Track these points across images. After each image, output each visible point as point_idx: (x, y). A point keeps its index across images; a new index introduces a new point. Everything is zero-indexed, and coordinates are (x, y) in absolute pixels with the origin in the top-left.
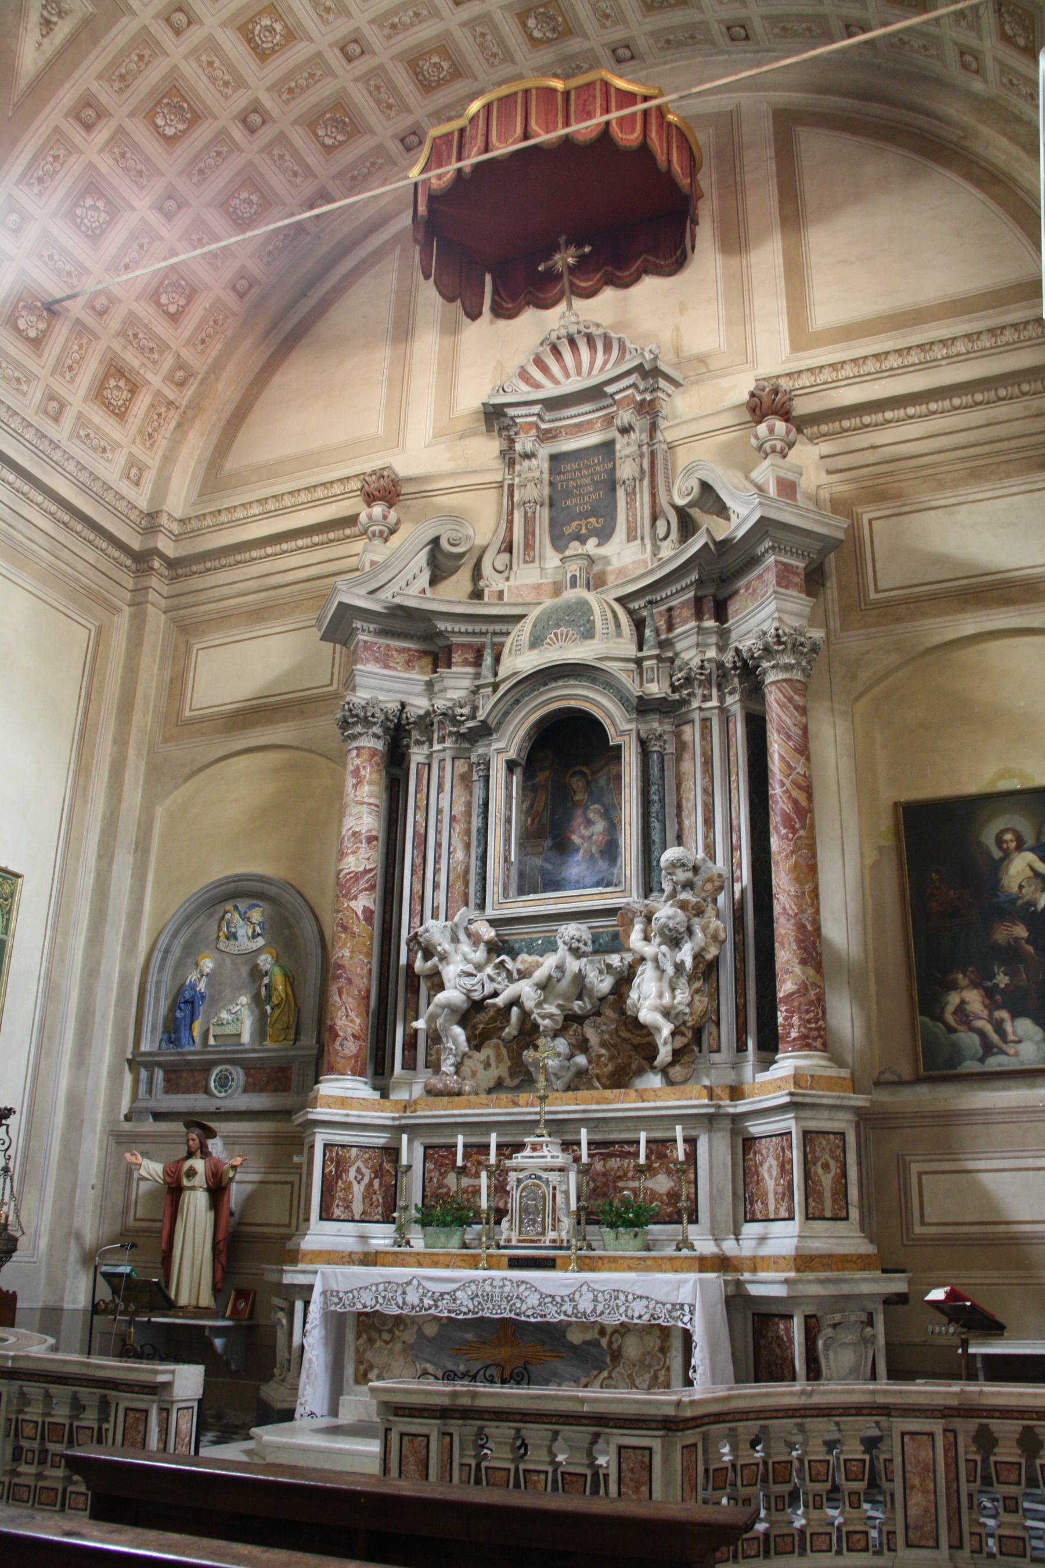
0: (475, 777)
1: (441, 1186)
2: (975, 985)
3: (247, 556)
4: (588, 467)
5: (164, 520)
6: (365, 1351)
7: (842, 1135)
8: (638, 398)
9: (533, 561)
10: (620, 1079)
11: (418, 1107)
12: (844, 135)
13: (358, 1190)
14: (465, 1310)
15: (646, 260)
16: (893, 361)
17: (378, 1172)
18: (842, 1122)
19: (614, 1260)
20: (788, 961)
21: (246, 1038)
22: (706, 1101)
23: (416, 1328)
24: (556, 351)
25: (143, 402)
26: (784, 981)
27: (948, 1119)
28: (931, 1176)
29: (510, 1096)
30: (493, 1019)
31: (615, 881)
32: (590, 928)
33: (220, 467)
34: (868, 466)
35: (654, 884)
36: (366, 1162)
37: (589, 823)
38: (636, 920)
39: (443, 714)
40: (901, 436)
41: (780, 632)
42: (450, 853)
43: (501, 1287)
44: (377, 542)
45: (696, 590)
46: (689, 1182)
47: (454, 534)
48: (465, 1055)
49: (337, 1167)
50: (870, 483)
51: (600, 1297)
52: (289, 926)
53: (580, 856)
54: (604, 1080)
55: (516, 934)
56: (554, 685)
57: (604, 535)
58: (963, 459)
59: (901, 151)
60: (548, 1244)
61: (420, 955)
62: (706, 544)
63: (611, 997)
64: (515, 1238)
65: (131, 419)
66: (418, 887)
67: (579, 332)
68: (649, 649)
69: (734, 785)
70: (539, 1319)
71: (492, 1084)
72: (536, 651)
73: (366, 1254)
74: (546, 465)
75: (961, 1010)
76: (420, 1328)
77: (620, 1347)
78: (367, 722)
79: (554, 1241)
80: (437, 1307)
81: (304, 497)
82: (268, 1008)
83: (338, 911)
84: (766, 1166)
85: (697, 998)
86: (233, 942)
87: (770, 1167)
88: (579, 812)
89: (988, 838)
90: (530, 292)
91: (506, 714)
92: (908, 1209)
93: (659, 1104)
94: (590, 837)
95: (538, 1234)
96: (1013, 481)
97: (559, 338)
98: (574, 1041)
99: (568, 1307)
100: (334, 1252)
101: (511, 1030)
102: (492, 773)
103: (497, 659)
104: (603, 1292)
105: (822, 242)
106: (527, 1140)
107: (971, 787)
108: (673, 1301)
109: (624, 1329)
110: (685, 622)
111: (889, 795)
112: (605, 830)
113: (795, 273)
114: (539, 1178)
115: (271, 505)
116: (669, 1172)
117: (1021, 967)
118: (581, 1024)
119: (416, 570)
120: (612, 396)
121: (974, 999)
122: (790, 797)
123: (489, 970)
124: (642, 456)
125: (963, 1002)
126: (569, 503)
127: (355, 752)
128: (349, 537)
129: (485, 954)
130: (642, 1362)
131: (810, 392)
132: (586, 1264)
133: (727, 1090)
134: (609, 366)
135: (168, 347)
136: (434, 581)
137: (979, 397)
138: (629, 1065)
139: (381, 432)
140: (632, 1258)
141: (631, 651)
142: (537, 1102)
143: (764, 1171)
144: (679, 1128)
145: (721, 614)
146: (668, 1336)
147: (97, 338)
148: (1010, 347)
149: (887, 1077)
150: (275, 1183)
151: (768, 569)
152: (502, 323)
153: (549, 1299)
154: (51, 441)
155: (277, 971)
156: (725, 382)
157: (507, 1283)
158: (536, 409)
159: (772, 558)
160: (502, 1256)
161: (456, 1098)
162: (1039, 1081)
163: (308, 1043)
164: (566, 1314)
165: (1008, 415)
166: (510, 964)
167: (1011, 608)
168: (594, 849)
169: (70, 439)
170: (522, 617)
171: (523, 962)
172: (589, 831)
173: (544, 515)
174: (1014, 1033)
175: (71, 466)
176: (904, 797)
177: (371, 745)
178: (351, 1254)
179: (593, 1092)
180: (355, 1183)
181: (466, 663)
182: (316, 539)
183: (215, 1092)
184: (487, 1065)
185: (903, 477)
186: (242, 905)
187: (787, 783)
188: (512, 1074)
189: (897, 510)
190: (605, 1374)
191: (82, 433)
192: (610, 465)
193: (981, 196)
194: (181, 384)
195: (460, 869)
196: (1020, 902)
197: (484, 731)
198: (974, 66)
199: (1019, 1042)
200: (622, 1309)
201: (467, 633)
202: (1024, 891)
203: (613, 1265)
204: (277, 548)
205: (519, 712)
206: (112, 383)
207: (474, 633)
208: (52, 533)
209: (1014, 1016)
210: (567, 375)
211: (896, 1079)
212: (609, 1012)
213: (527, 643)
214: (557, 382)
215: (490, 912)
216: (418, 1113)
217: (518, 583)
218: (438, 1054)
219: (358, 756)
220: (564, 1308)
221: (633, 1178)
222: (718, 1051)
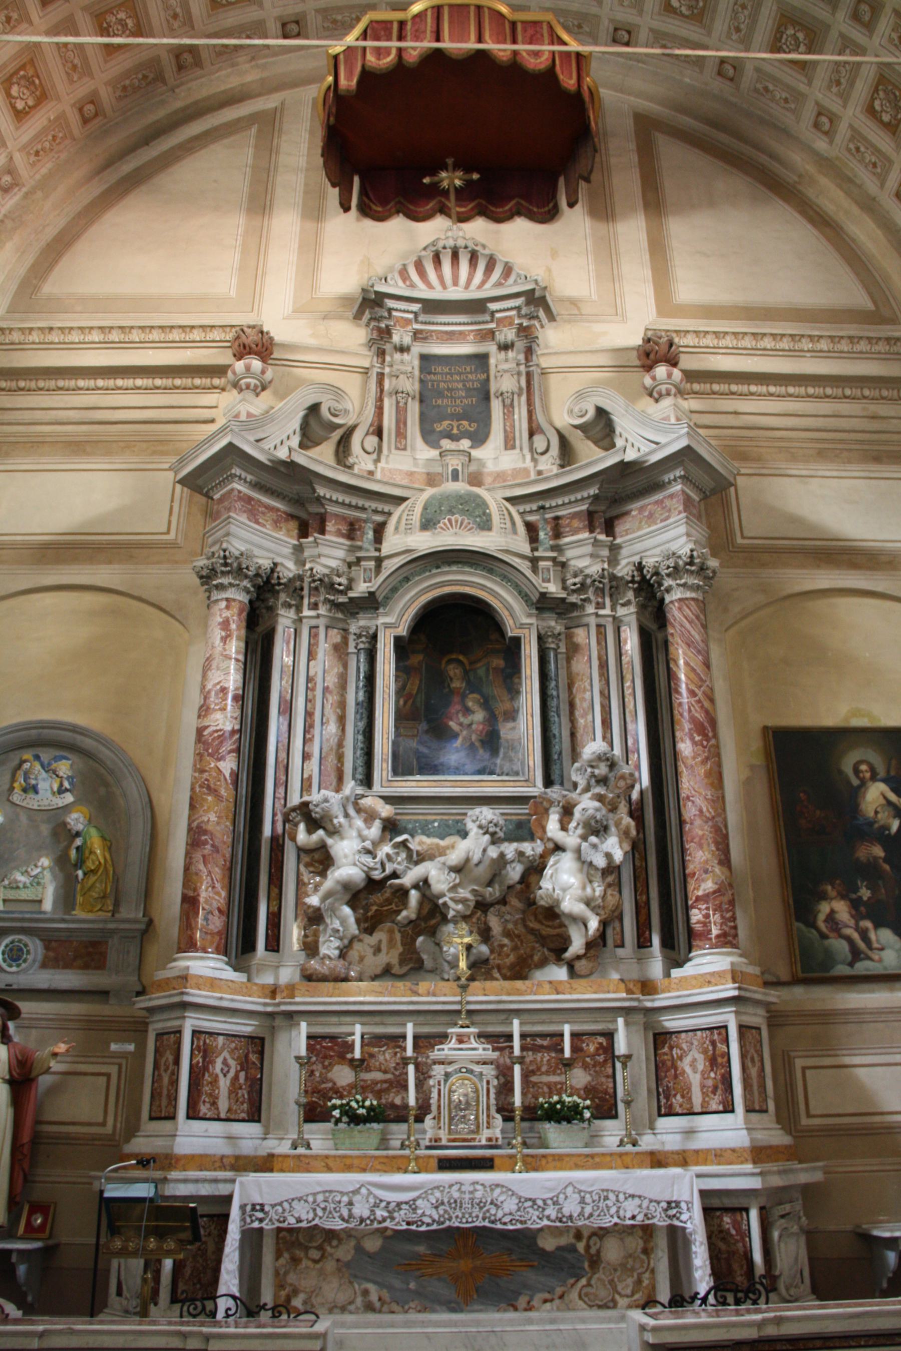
0: (351, 649)
1: (324, 1080)
2: (843, 897)
3: (72, 383)
4: (460, 374)
6: (286, 1273)
7: (758, 1029)
10: (519, 971)
11: (297, 992)
12: (697, 151)
13: (224, 1084)
14: (427, 1220)
15: (518, 203)
16: (767, 343)
17: (245, 1064)
19: (559, 1158)
20: (706, 862)
21: (48, 905)
22: (624, 995)
23: (353, 1243)
24: (437, 259)
27: (827, 1017)
28: (813, 1071)
29: (408, 984)
30: (388, 901)
31: (498, 771)
32: (502, 814)
33: (37, 288)
34: (732, 428)
35: (555, 777)
36: (232, 1052)
37: (467, 711)
38: (552, 810)
39: (320, 580)
40: (759, 408)
41: (695, 553)
42: (322, 724)
43: (471, 1192)
44: (249, 395)
45: (590, 504)
46: (608, 1077)
49: (204, 1058)
50: (733, 443)
51: (588, 1199)
52: (106, 785)
53: (458, 743)
54: (504, 971)
55: (411, 814)
56: (447, 569)
57: (480, 438)
58: (817, 440)
59: (749, 179)
60: (484, 1142)
61: (302, 827)
63: (519, 886)
64: (444, 1135)
67: (466, 247)
68: (545, 550)
69: (628, 692)
70: (519, 1226)
71: (378, 971)
73: (237, 1158)
74: (416, 363)
75: (831, 917)
76: (359, 1243)
77: (598, 1252)
78: (239, 572)
79: (490, 1139)
80: (393, 1219)
81: (155, 335)
83: (202, 771)
84: (687, 1060)
85: (609, 892)
86: (31, 795)
88: (456, 699)
89: (847, 766)
90: (400, 202)
91: (394, 590)
92: (795, 1103)
93: (575, 996)
94: (470, 725)
95: (473, 1132)
96: (854, 467)
97: (444, 248)
99: (551, 1211)
100: (206, 1156)
101: (409, 912)
102: (380, 645)
103: (378, 537)
104: (591, 1193)
105: (681, 230)
106: (450, 1031)
107: (829, 720)
108: (668, 1199)
109: (601, 1233)
110: (576, 532)
111: (758, 720)
113: (658, 249)
114: (470, 1071)
115: (115, 336)
116: (585, 1067)
117: (880, 882)
118: (485, 912)
120: (493, 313)
121: (842, 909)
122: (702, 707)
125: (832, 912)
126: (439, 402)
127: (223, 604)
128: (197, 388)
129: (380, 832)
130: (623, 1265)
131: (695, 351)
132: (533, 1164)
133: (639, 985)
134: (488, 285)
136: (302, 446)
137: (829, 391)
138: (532, 956)
139: (233, 293)
140: (579, 1155)
141: (525, 548)
142: (459, 990)
143: (685, 1065)
144: (516, 1022)
145: (609, 530)
146: (651, 1236)
148: (862, 356)
150: (93, 1074)
151: (671, 496)
152: (368, 223)
153: (530, 1203)
155: (93, 832)
157: (478, 1187)
158: (416, 307)
159: (679, 487)
160: (430, 1157)
162: (898, 985)
163: (132, 916)
164: (548, 1218)
165: (850, 412)
167: (859, 572)
168: (474, 737)
171: (421, 843)
172: (468, 720)
173: (414, 410)
174: (878, 941)
177: (241, 599)
178: (223, 1157)
179: (495, 983)
180: (221, 1076)
181: (339, 533)
182: (158, 382)
184: (377, 950)
185: (762, 444)
186: (46, 755)
187: (700, 693)
188: (402, 962)
189: (757, 471)
190: (583, 1281)
192: (484, 376)
193: (815, 232)
195: (334, 741)
196: (876, 826)
197: (372, 603)
198: (826, 127)
199: (882, 949)
200: (613, 1210)
201: (343, 504)
202: (879, 816)
203: (558, 1164)
204: (111, 383)
205: (408, 590)
207: (350, 506)
209: (877, 925)
210: (455, 283)
211: (775, 980)
212: (514, 902)
213: (418, 524)
216: (297, 999)
217: (391, 466)
218: (316, 935)
219: (227, 607)
220: (547, 1213)
221: (547, 1073)
222: (622, 946)
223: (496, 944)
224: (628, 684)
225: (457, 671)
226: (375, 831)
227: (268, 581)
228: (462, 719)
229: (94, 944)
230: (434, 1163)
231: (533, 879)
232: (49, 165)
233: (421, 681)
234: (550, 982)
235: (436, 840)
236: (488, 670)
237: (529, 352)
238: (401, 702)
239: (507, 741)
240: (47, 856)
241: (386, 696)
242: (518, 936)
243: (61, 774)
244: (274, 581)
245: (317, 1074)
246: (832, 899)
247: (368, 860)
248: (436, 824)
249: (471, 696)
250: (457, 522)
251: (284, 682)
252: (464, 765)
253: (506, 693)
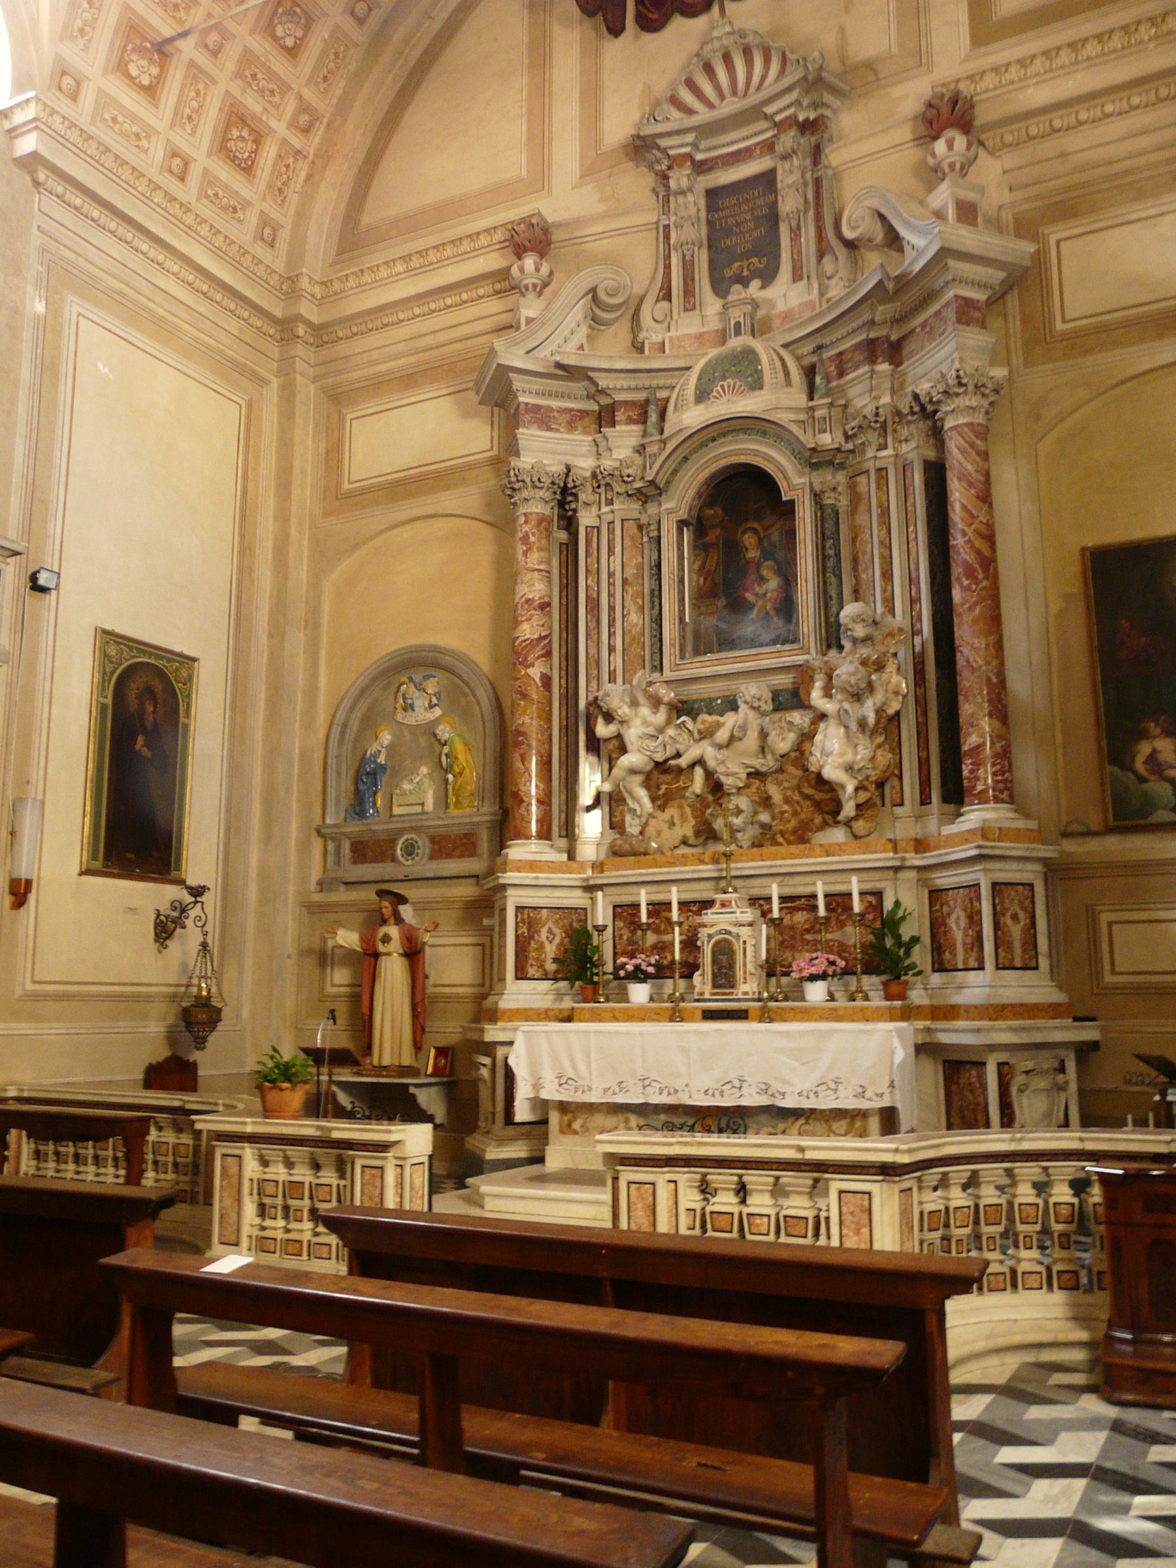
5: (305, 283)
7: (1031, 886)
8: (801, 118)
9: (694, 309)
10: (801, 836)
11: (605, 867)
18: (1030, 873)
22: (891, 854)
25: (270, 151)
26: (969, 734)
33: (357, 222)
37: (762, 580)
41: (961, 373)
42: (624, 616)
47: (611, 284)
48: (651, 816)
49: (529, 929)
52: (465, 695)
53: (754, 614)
54: (787, 836)
57: (768, 276)
62: (880, 282)
65: (259, 172)
66: (593, 651)
68: (820, 398)
69: (912, 536)
72: (702, 406)
74: (702, 202)
75: (1153, 759)
82: (450, 777)
83: (516, 679)
84: (953, 917)
85: (879, 752)
86: (410, 712)
87: (958, 918)
91: (675, 472)
92: (1098, 959)
93: (844, 858)
94: (764, 595)
98: (757, 799)
110: (857, 367)
112: (779, 586)
114: (729, 933)
118: (763, 782)
119: (573, 325)
122: (972, 546)
123: (671, 731)
124: (805, 184)
125: (1154, 752)
133: (912, 843)
135: (289, 88)
139: (524, 173)
141: (801, 399)
143: (951, 922)
144: (854, 879)
147: (214, 82)
149: (1076, 827)
154: (182, 204)
156: (897, 91)
158: (690, 138)
160: (697, 1008)
161: (642, 858)
166: (690, 725)
169: (198, 200)
170: (688, 369)
171: (704, 722)
175: (204, 230)
176: (1092, 541)
180: (547, 943)
181: (630, 421)
183: (402, 860)
184: (672, 824)
187: (970, 532)
188: (697, 834)
191: (210, 192)
194: (306, 130)
203: (805, 1016)
206: (235, 133)
208: (191, 303)
211: (1084, 830)
212: (791, 769)
214: (711, 106)
215: (668, 674)
219: (526, 522)
222: (902, 804)
223: (777, 811)
224: (911, 529)
225: (752, 540)
226: (661, 717)
227: (565, 490)
229: (466, 836)
230: (699, 1014)
231: (806, 746)
232: (342, 84)
234: (821, 845)
237: (817, 153)
238: (702, 580)
240: (426, 764)
242: (798, 802)
243: (430, 691)
244: (570, 485)
245: (625, 937)
246: (1155, 737)
247: (652, 744)
251: (589, 581)
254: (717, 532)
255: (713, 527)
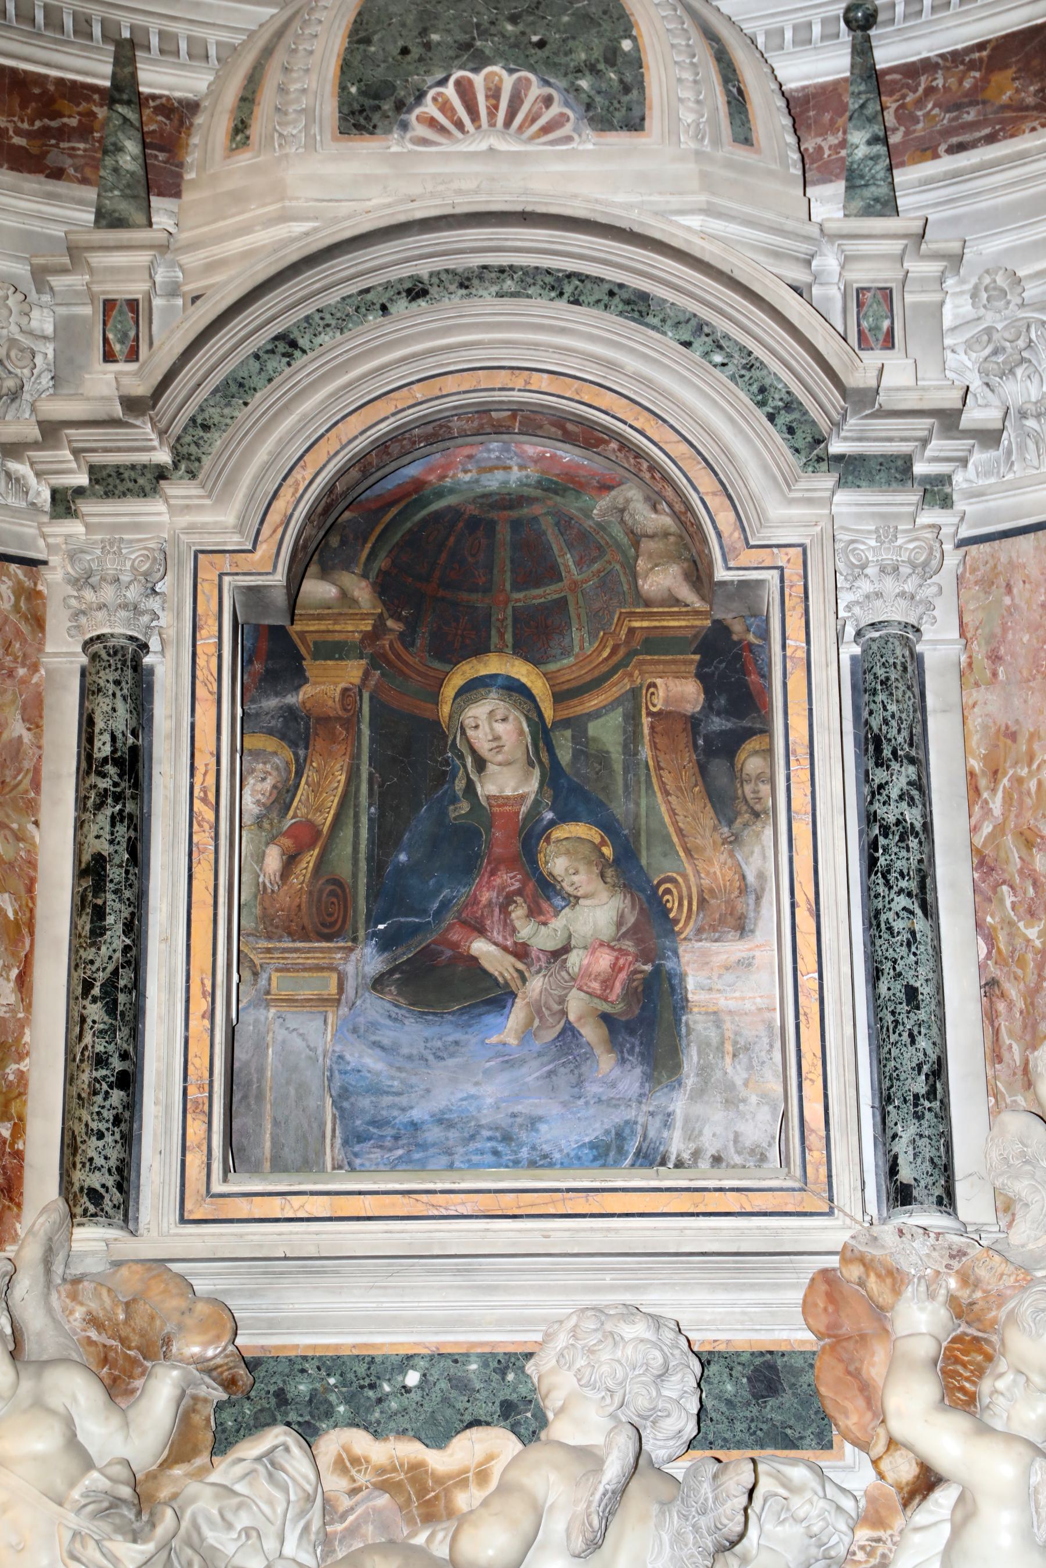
31: (677, 1145)
72: (366, 146)
91: (236, 389)
168: (576, 1005)
213: (329, 108)
225: (500, 728)
228: (526, 930)
233: (353, 775)
235: (410, 1450)
236: (632, 718)
238: (273, 860)
239: (716, 1017)
241: (204, 837)
248: (412, 1378)
249: (560, 832)
250: (494, 94)
252: (533, 1122)
253: (708, 817)
254: (352, 671)
255: (332, 650)
